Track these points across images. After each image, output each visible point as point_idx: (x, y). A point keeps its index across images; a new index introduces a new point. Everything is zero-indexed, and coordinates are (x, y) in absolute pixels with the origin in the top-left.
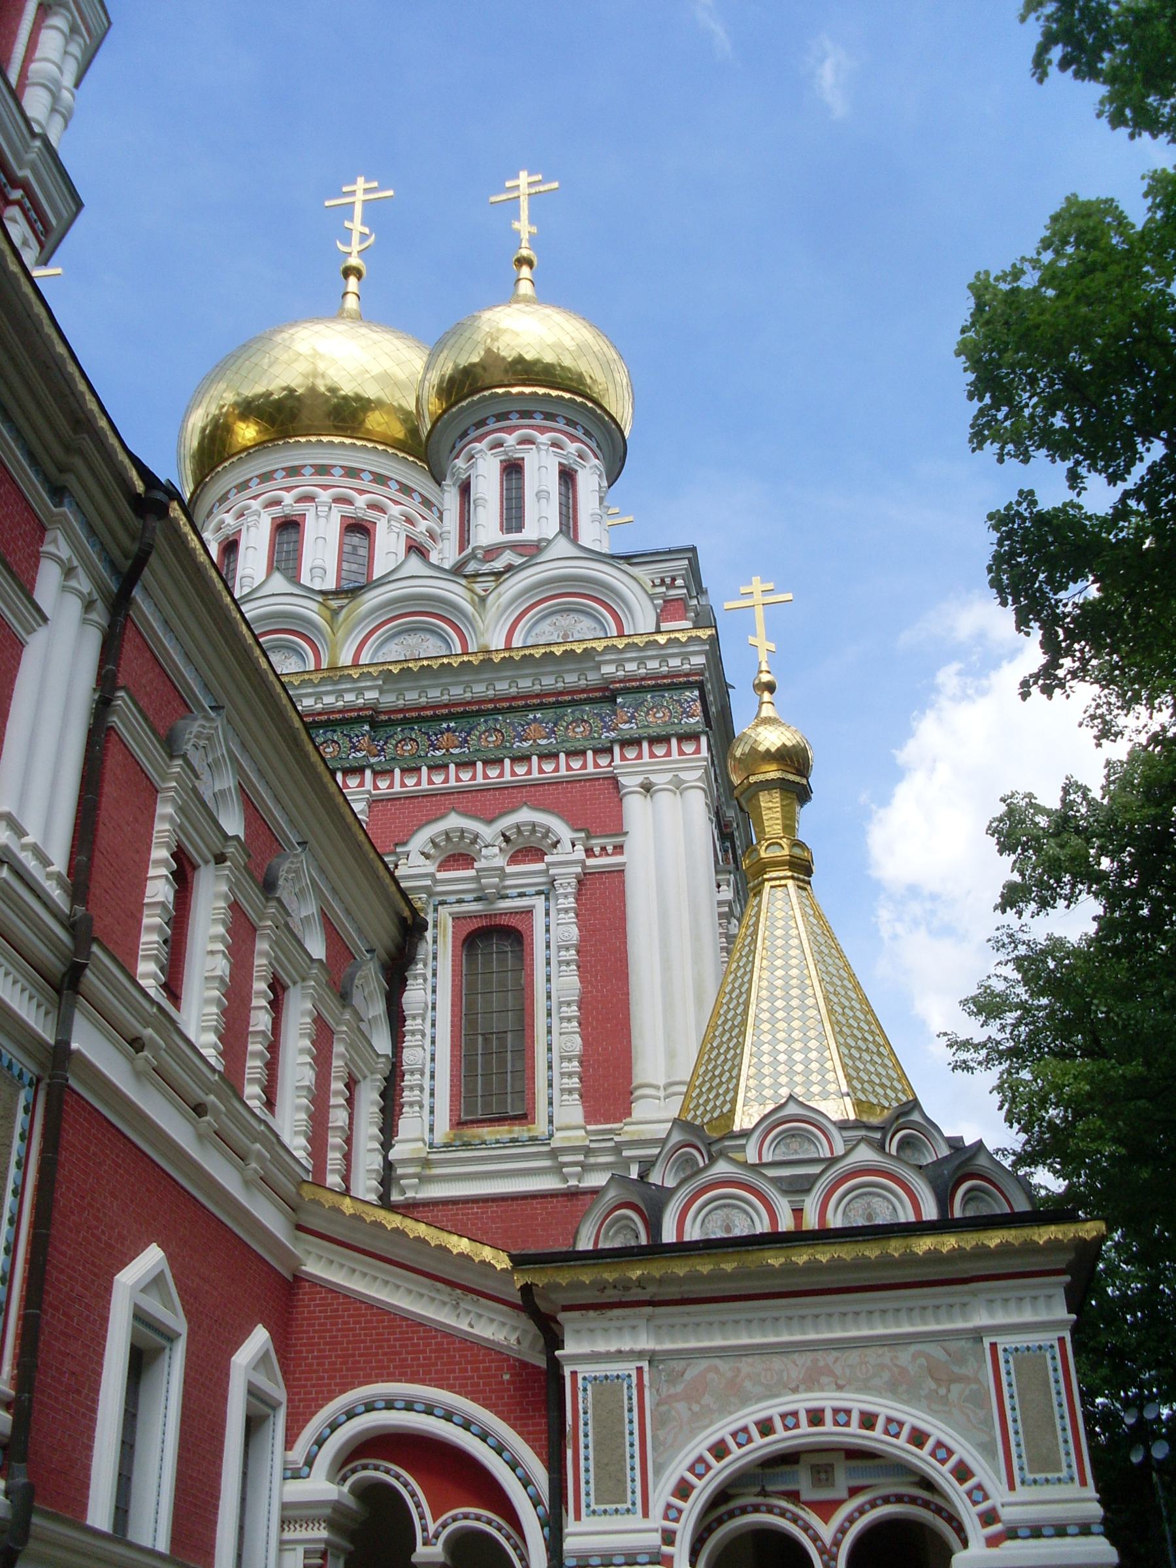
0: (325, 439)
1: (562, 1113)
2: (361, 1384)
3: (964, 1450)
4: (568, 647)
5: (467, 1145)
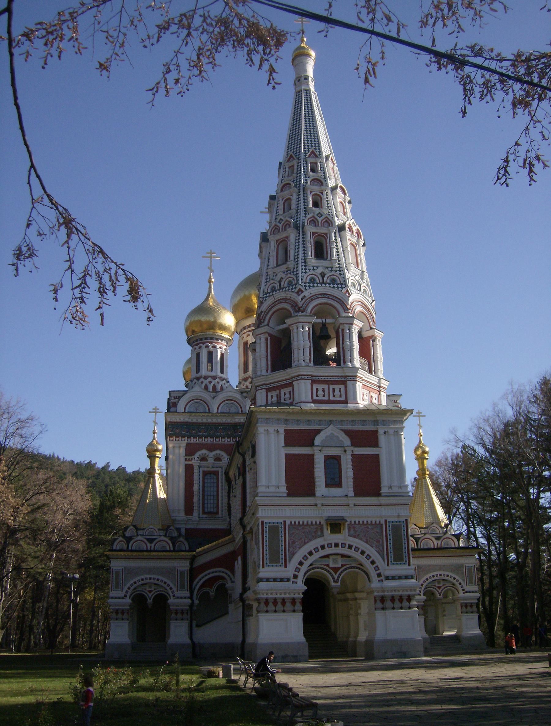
3: (172, 585)
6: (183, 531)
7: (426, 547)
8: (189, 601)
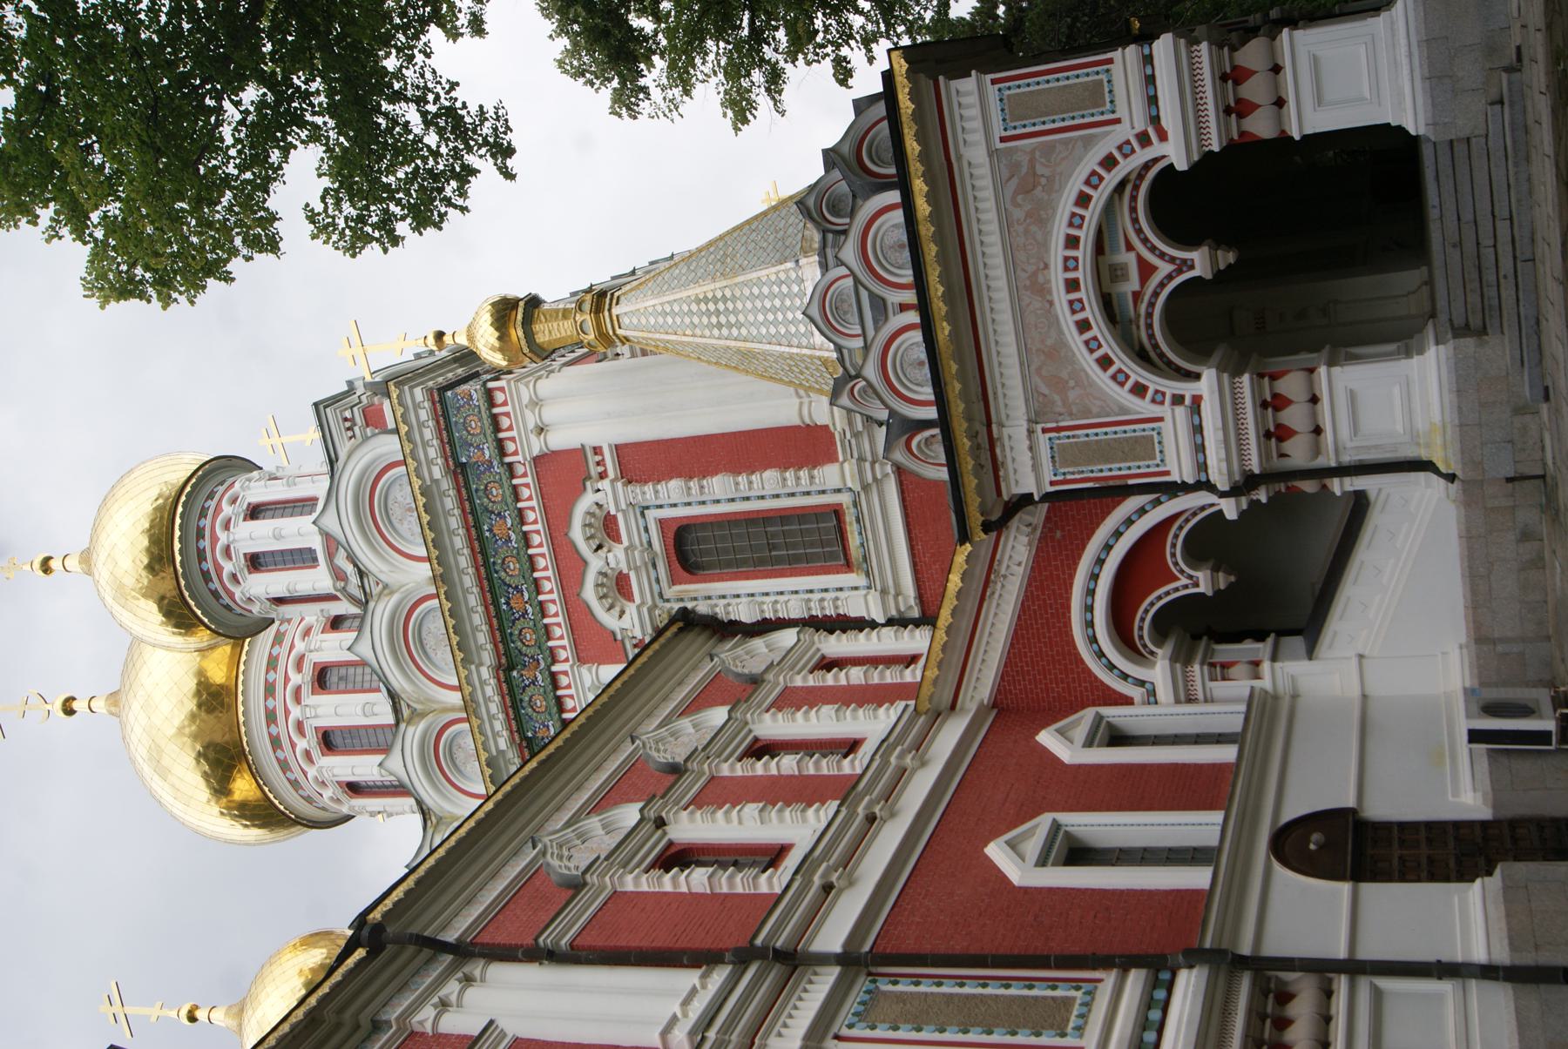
0: (241, 719)
1: (829, 482)
2: (1075, 648)
3: (1091, 162)
4: (422, 509)
5: (865, 559)
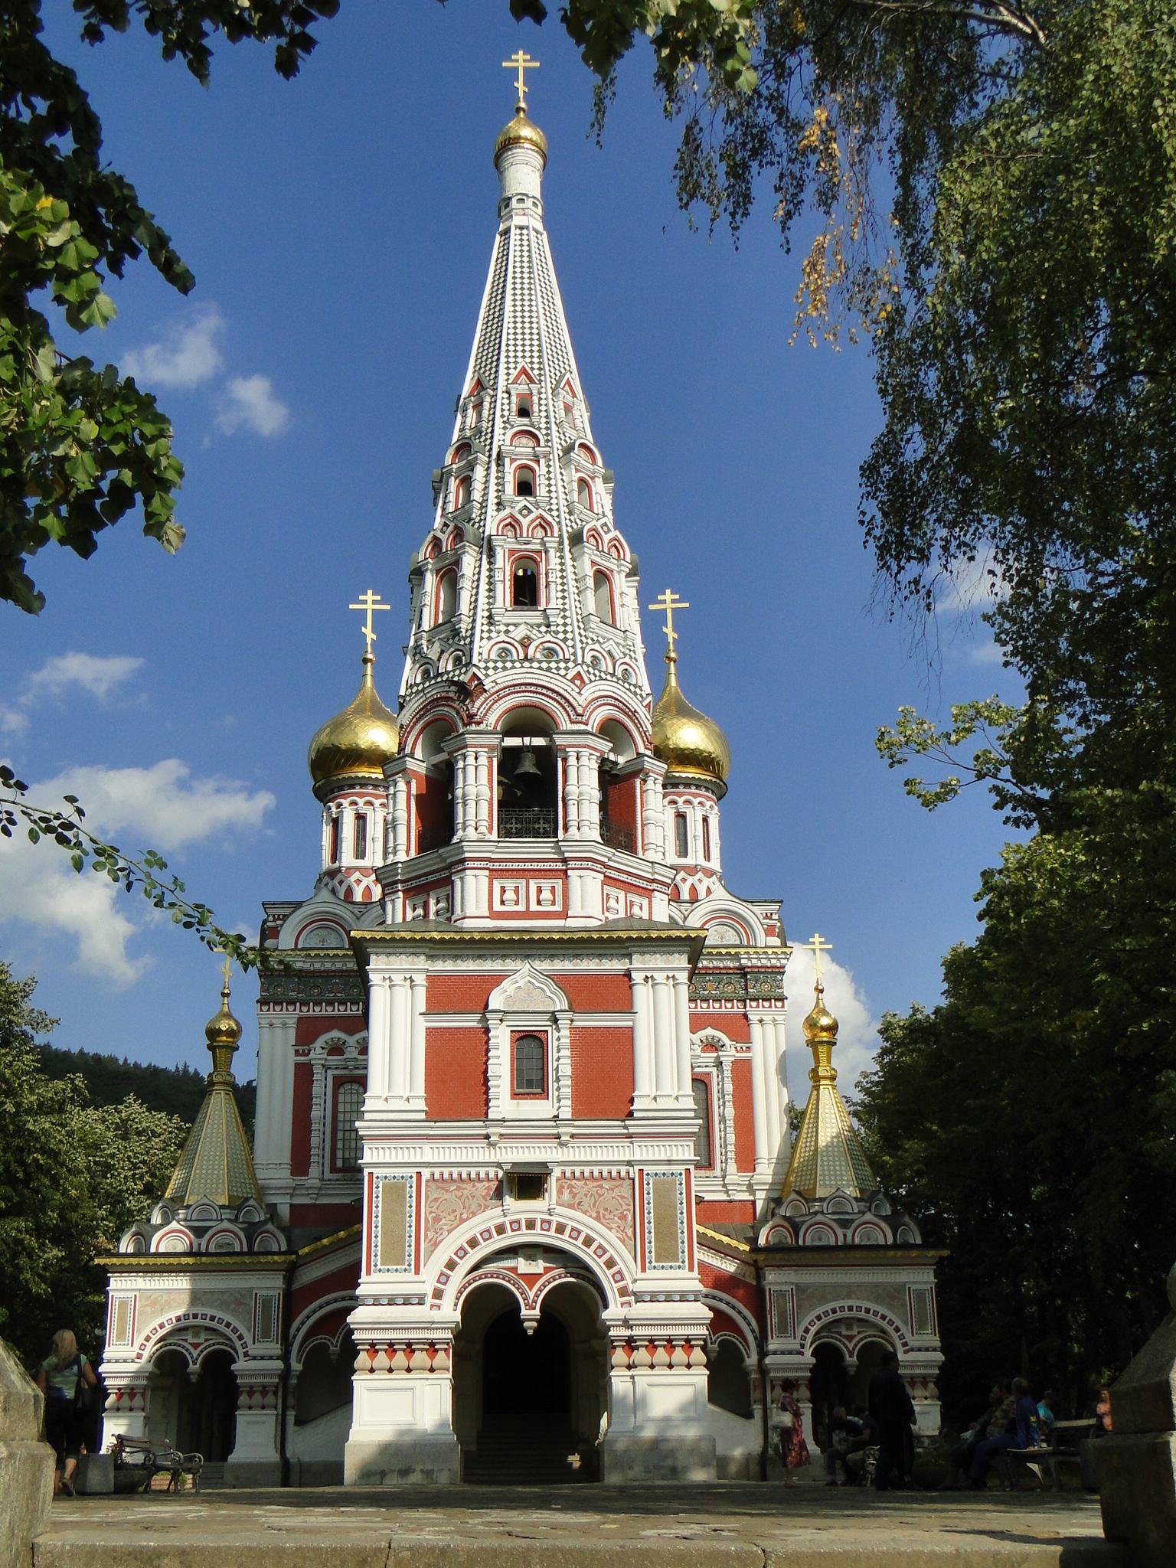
3: (242, 1330)
6: (284, 1211)
7: (817, 1243)
8: (279, 1365)
